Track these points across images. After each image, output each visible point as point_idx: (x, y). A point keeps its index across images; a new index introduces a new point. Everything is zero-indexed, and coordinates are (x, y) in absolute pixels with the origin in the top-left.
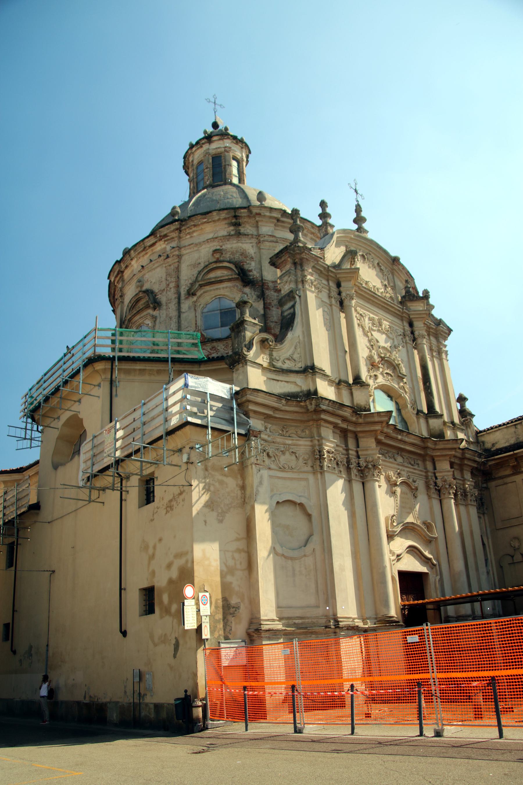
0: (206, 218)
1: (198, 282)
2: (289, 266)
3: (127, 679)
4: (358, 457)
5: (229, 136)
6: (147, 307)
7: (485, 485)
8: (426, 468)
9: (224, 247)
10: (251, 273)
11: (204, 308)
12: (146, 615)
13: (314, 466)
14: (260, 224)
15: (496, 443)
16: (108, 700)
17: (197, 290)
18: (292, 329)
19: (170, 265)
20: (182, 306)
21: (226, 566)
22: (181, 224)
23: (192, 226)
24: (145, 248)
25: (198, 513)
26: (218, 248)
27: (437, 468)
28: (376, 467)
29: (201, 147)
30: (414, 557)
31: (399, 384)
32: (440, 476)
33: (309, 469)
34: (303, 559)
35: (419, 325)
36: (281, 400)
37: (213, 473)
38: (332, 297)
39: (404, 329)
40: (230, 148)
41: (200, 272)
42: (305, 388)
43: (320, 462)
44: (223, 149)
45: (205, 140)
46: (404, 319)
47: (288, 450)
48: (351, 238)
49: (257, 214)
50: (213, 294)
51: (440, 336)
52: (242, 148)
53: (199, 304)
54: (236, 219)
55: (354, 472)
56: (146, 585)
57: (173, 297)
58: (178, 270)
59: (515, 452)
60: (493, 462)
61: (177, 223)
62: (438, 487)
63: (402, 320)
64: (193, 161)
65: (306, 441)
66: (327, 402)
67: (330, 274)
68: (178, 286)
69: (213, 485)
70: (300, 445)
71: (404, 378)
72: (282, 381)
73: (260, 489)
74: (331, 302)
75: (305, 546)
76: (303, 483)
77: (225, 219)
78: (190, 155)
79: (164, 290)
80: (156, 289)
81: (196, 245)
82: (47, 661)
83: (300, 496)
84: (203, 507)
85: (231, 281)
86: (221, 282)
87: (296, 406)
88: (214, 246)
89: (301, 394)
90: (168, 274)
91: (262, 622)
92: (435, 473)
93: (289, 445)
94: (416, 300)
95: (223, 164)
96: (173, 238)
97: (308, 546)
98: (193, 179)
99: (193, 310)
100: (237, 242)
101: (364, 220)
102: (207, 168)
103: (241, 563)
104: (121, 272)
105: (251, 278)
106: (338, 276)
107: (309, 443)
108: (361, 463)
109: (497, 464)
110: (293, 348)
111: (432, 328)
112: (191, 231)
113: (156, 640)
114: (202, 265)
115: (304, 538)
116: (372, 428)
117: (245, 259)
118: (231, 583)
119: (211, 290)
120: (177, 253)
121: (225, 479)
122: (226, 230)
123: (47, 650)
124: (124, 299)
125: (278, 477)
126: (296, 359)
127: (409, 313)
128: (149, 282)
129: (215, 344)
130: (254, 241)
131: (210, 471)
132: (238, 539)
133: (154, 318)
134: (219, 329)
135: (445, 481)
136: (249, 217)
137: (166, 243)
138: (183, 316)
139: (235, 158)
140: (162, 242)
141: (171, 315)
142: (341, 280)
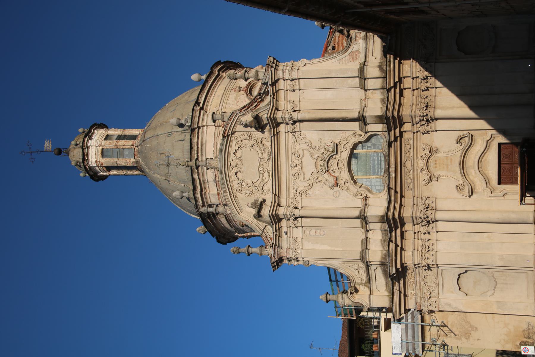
73: (454, 307)
76: (444, 272)
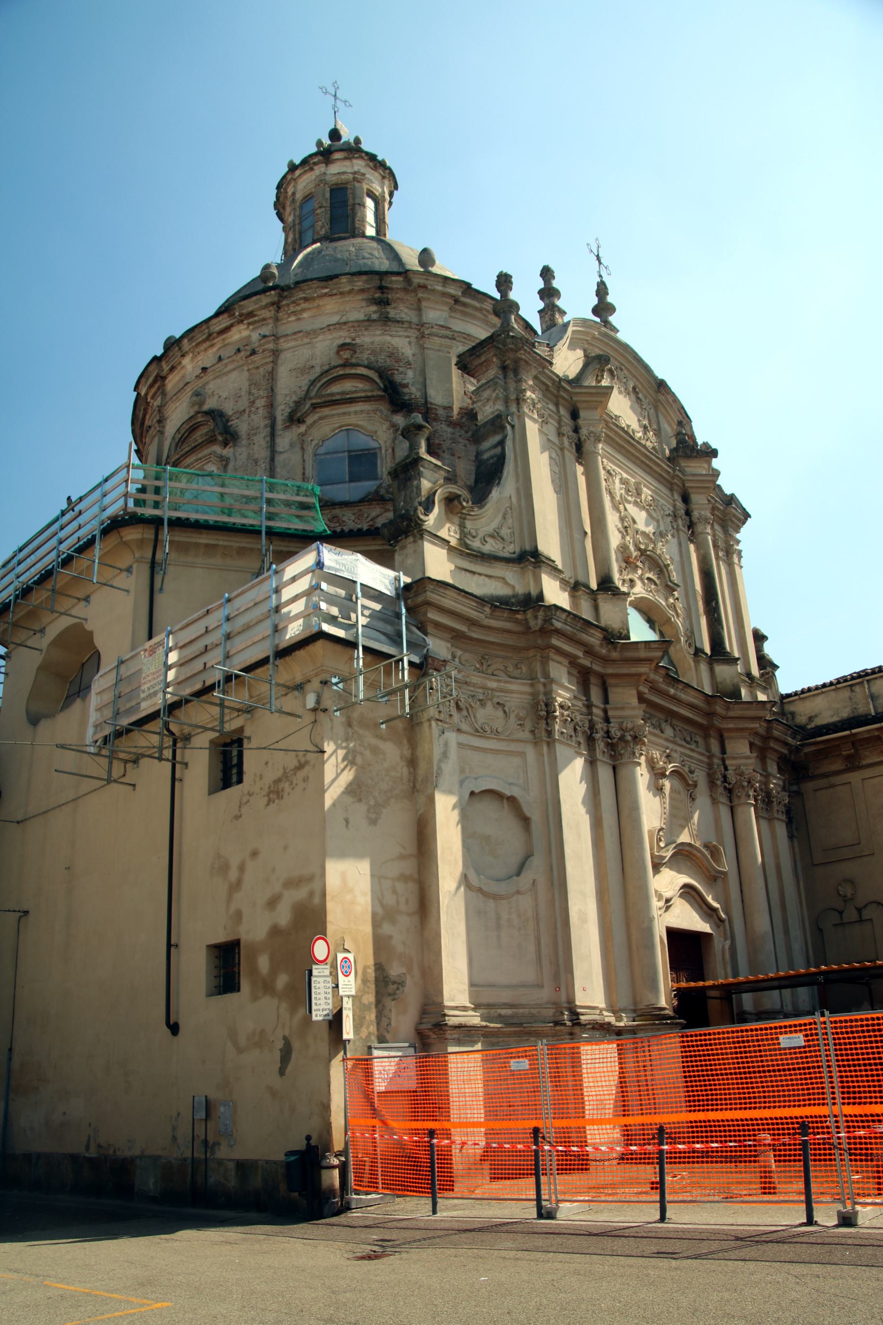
0: (327, 288)
1: (311, 399)
2: (493, 372)
3: (179, 1114)
4: (607, 720)
5: (363, 155)
6: (211, 440)
7: (795, 788)
8: (708, 750)
9: (358, 341)
10: (406, 390)
11: (318, 446)
12: (220, 994)
13: (536, 731)
14: (424, 304)
15: (816, 716)
16: (137, 1152)
17: (306, 414)
18: (499, 484)
19: (257, 368)
20: (278, 440)
21: (382, 906)
22: (280, 296)
23: (301, 299)
24: (210, 335)
25: (334, 805)
26: (348, 341)
27: (728, 751)
28: (637, 740)
29: (312, 169)
30: (691, 905)
31: (666, 599)
32: (732, 765)
33: (526, 735)
34: (515, 898)
35: (699, 500)
36: (484, 606)
37: (361, 731)
38: (564, 435)
39: (674, 506)
40: (364, 175)
41: (313, 383)
42: (520, 590)
43: (547, 724)
44: (351, 176)
45: (320, 158)
46: (675, 487)
47: (491, 700)
48: (594, 338)
49: (420, 286)
50: (336, 422)
51: (730, 523)
52: (384, 178)
53: (310, 439)
54: (382, 293)
55: (600, 746)
56: (221, 937)
57: (262, 424)
58: (272, 376)
59: (854, 731)
60: (813, 748)
61: (273, 292)
62: (729, 784)
63: (671, 490)
64: (294, 194)
65: (523, 684)
66: (564, 616)
67: (562, 393)
68: (271, 406)
69: (361, 753)
70: (512, 692)
71: (675, 590)
72: (480, 574)
73: (443, 766)
74: (562, 443)
75: (518, 874)
76: (517, 760)
77: (362, 291)
78: (289, 183)
79: (244, 411)
80: (229, 408)
81: (308, 333)
82: (9, 1078)
83: (510, 784)
84: (343, 793)
85: (370, 401)
86: (351, 402)
87: (509, 620)
88: (340, 337)
89: (513, 600)
90: (253, 383)
91: (447, 1012)
92: (723, 760)
93: (493, 690)
94: (696, 457)
95: (351, 201)
96: (264, 319)
97: (523, 875)
98: (294, 225)
99: (298, 448)
100: (383, 334)
101: (611, 309)
102: (320, 207)
103: (407, 902)
104: (161, 378)
105: (407, 398)
106: (574, 399)
107: (527, 689)
108: (613, 731)
109: (819, 752)
110: (500, 517)
111: (719, 509)
112: (299, 308)
113: (243, 1041)
114: (318, 371)
115: (514, 861)
116: (634, 670)
117: (395, 364)
118: (390, 937)
119: (333, 415)
120: (271, 346)
121: (381, 745)
122: (363, 310)
123: (10, 1059)
124: (164, 427)
125: (470, 746)
126: (505, 537)
127: (684, 478)
128: (216, 397)
129: (337, 511)
130: (413, 333)
131: (356, 728)
132: (402, 857)
133: (225, 462)
134: (346, 485)
135: (741, 774)
136: (405, 290)
137: (251, 327)
138: (279, 459)
139: (371, 194)
140: (242, 327)
141: (256, 456)
142: (579, 405)
